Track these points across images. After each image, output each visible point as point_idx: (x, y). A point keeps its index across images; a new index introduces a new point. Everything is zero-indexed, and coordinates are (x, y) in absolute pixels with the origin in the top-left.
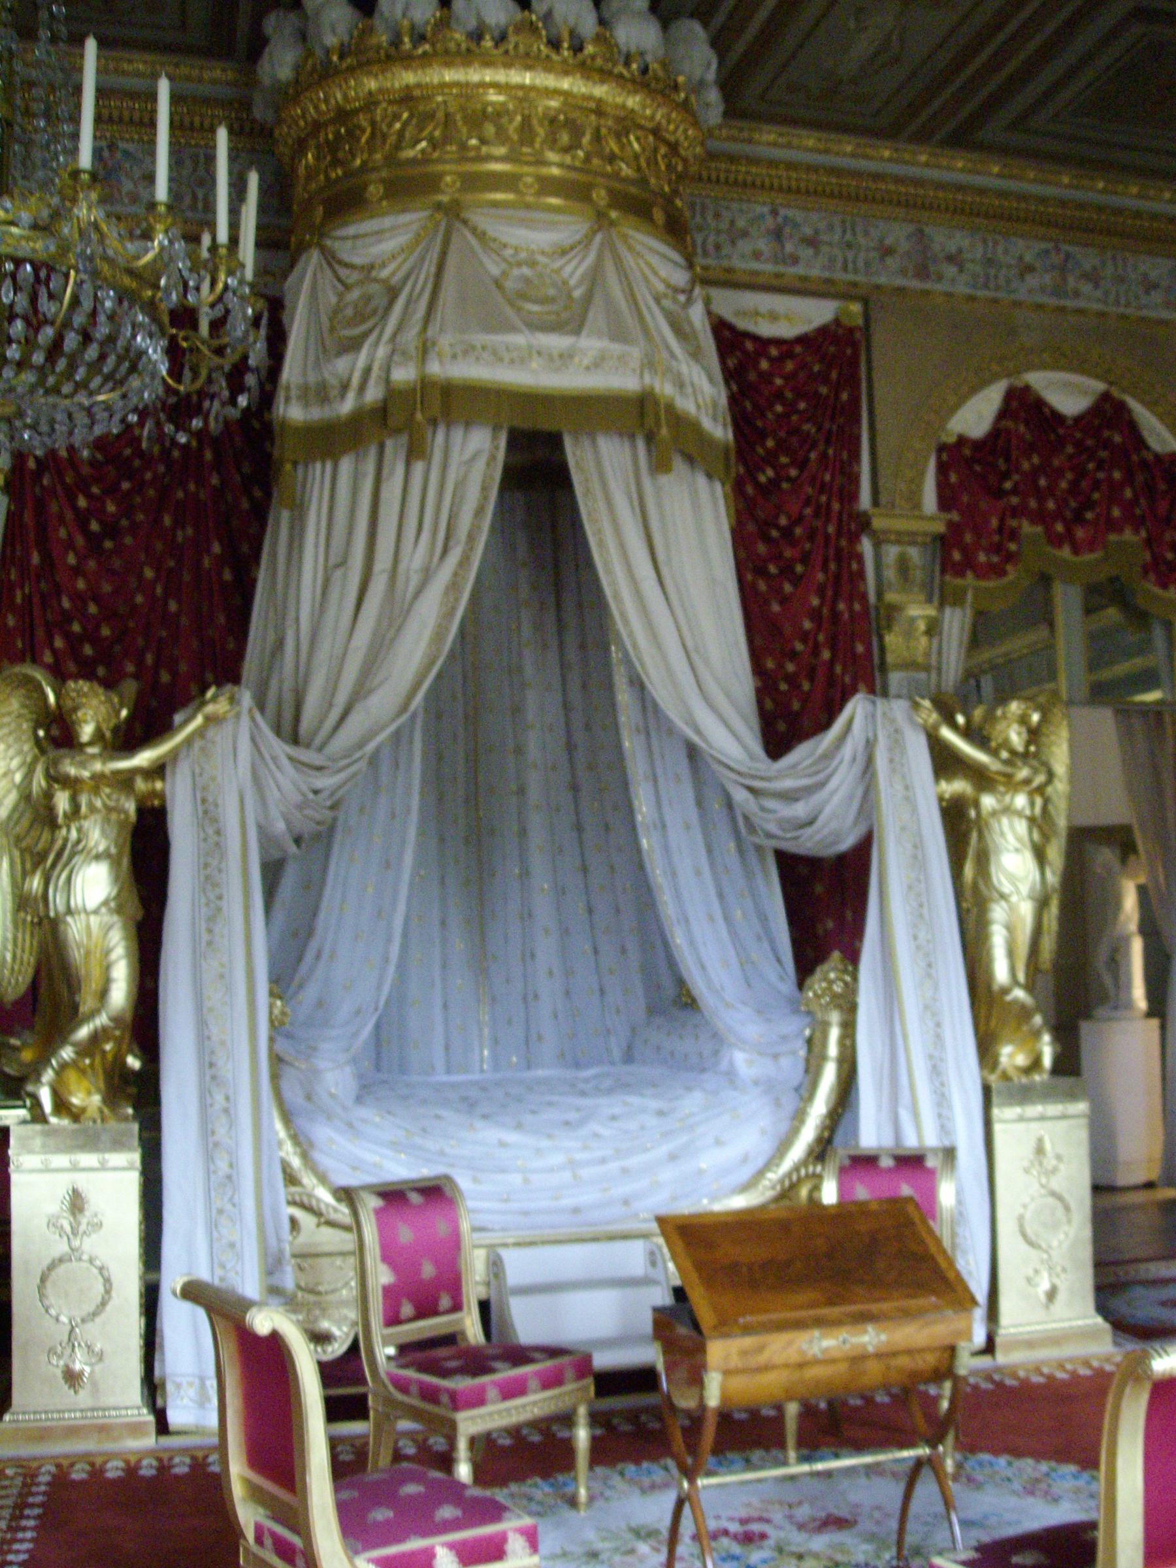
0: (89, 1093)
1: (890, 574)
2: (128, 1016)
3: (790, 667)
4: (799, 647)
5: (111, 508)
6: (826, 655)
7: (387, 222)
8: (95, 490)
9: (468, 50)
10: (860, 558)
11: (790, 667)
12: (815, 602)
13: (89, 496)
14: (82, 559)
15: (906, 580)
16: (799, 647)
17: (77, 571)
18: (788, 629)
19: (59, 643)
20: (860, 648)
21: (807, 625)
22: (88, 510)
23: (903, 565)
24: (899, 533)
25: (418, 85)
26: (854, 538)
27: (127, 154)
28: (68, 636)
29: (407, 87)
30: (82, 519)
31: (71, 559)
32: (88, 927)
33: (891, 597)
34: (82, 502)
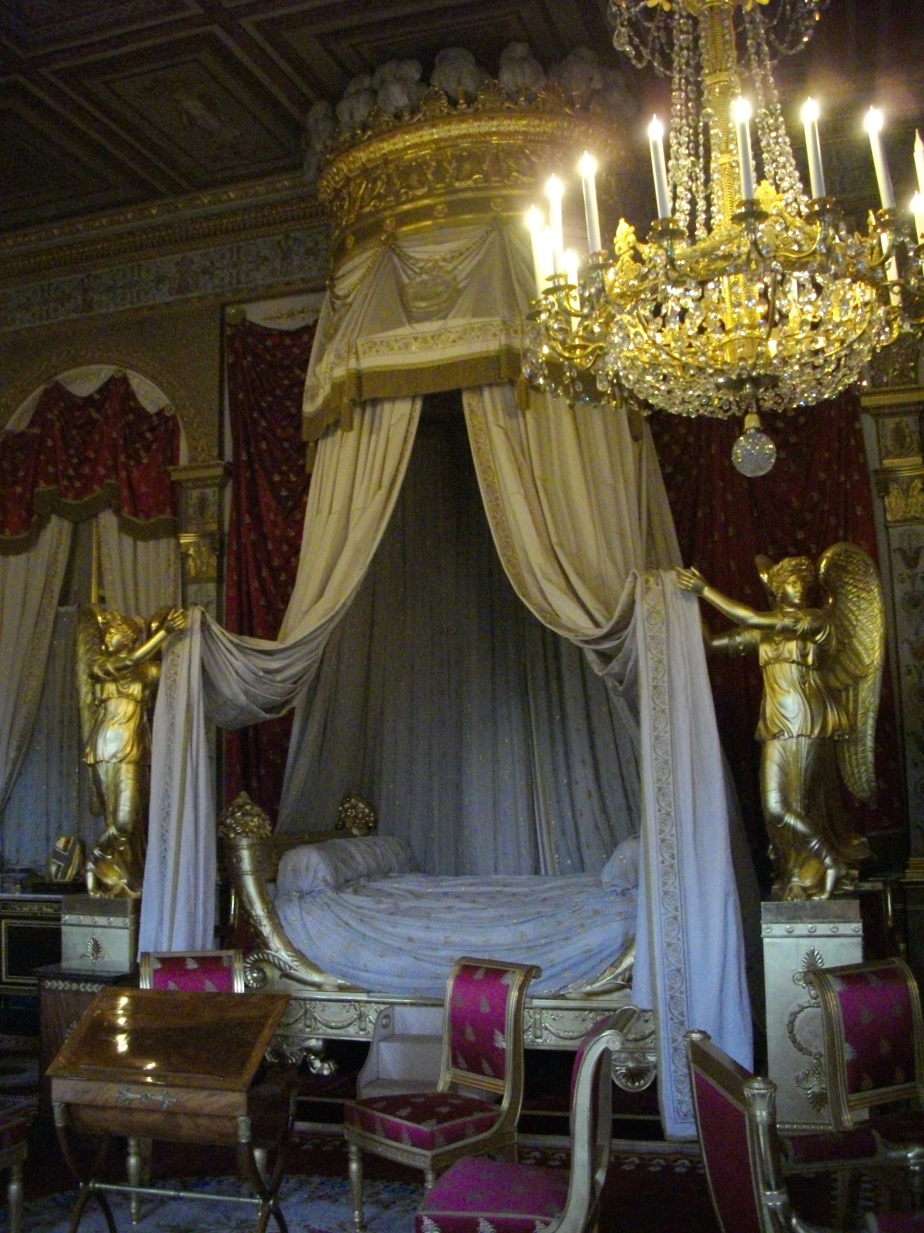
0: (120, 878)
1: (889, 443)
2: (130, 828)
3: (800, 535)
4: (808, 516)
5: (293, 478)
6: (833, 521)
7: (357, 261)
8: (284, 468)
9: (449, 114)
10: (859, 434)
11: (800, 535)
12: (822, 476)
13: (281, 473)
14: (276, 515)
15: (902, 446)
16: (808, 516)
17: (275, 524)
18: (795, 502)
19: (265, 573)
20: (859, 512)
21: (815, 496)
22: (280, 482)
23: (899, 435)
24: (891, 406)
25: (391, 152)
26: (855, 417)
27: (295, 239)
28: (271, 568)
29: (384, 154)
30: (274, 489)
31: (272, 517)
32: (107, 770)
33: (887, 463)
34: (277, 478)
